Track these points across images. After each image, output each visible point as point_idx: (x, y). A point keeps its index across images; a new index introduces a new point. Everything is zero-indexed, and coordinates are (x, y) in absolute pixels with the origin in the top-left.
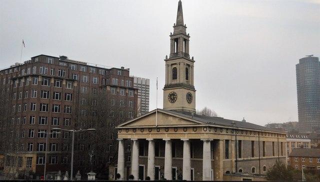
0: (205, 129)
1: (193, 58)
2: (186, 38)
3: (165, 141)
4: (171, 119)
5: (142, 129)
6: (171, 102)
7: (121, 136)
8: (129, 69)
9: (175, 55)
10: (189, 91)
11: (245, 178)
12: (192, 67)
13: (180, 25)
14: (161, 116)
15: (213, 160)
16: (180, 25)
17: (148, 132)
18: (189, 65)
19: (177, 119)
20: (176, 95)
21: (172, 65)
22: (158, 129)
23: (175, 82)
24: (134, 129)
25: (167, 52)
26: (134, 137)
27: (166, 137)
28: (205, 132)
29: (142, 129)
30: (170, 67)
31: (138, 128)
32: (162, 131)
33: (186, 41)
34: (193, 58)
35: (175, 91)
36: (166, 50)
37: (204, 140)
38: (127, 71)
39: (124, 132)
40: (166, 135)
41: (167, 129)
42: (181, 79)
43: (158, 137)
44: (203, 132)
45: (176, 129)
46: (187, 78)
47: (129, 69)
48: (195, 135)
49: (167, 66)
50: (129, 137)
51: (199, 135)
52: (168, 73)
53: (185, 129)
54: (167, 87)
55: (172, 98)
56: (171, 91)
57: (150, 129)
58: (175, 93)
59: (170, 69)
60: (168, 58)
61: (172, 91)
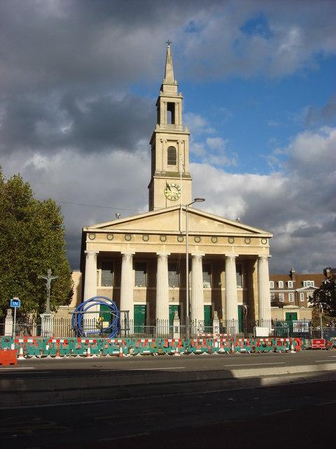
0: (264, 241)
17: (161, 243)
23: (173, 169)
24: (128, 234)
28: (263, 245)
43: (180, 250)
44: (261, 245)
48: (248, 250)
51: (256, 250)
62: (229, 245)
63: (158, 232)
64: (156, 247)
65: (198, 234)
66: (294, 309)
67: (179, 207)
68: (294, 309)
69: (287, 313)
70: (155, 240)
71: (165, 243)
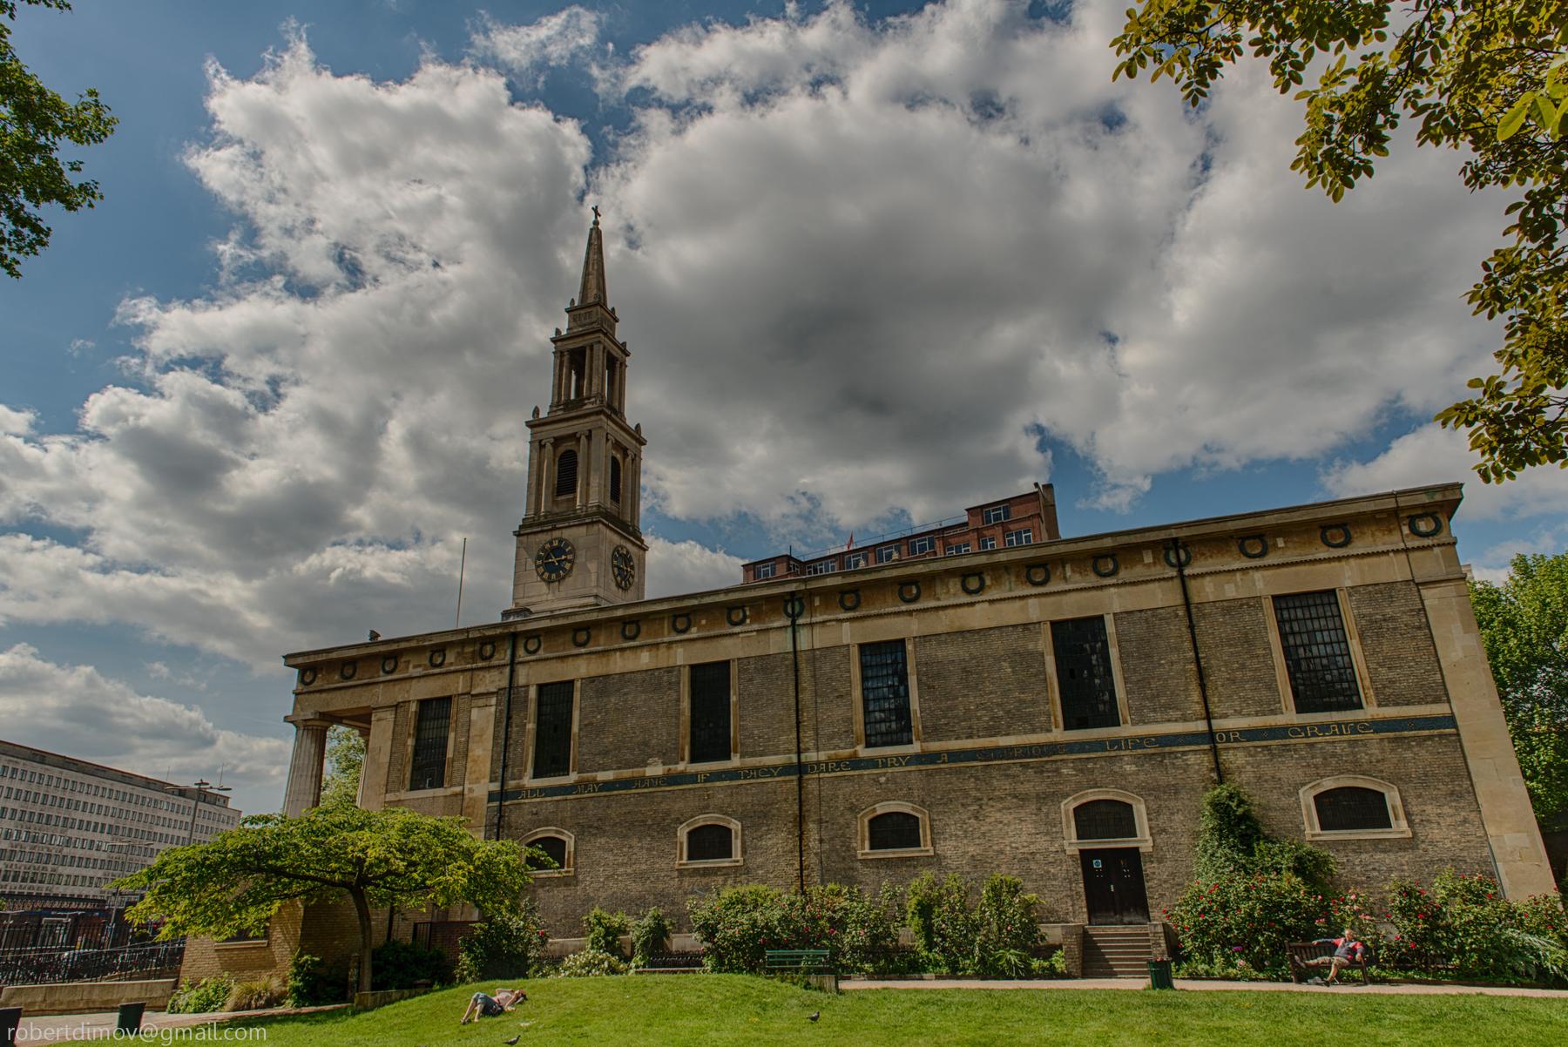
1: (638, 426)
2: (616, 352)
6: (549, 582)
9: (566, 406)
10: (623, 542)
12: (636, 459)
18: (625, 451)
20: (573, 552)
21: (558, 441)
33: (615, 364)
34: (638, 426)
35: (566, 534)
42: (593, 490)
46: (615, 495)
49: (538, 445)
52: (539, 484)
55: (554, 564)
58: (567, 545)
60: (543, 414)
61: (556, 534)
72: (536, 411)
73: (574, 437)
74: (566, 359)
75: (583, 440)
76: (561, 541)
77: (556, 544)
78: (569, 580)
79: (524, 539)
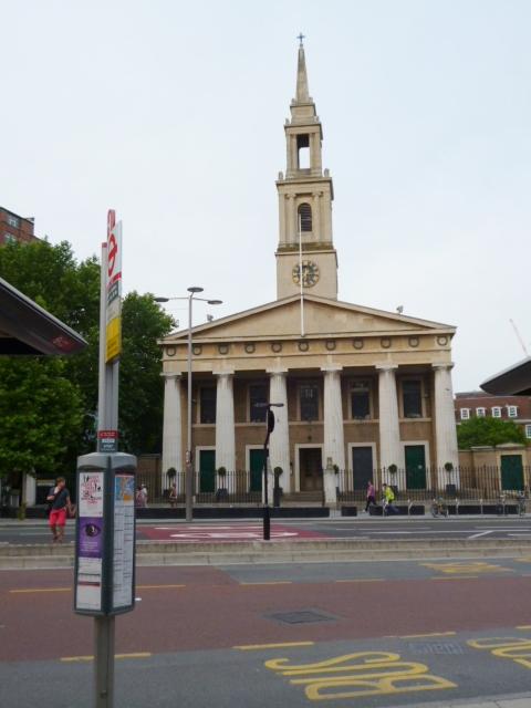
3: (325, 373)
4: (342, 317)
5: (247, 344)
7: (172, 367)
8: (33, 219)
11: (505, 453)
13: (302, 104)
14: (311, 310)
15: (429, 420)
16: (302, 104)
17: (273, 354)
19: (361, 319)
21: (299, 195)
22: (304, 342)
23: (303, 238)
24: (223, 346)
25: (281, 165)
26: (224, 367)
27: (331, 364)
28: (444, 348)
29: (250, 345)
30: (291, 199)
31: (236, 343)
32: (313, 349)
36: (275, 156)
37: (444, 365)
38: (29, 223)
39: (180, 354)
40: (330, 358)
41: (330, 342)
44: (437, 347)
45: (358, 341)
47: (33, 219)
50: (204, 367)
51: (428, 355)
53: (386, 340)
54: (284, 250)
56: (306, 258)
57: (277, 344)
59: (293, 206)
62: (385, 350)
63: (346, 336)
64: (267, 360)
65: (330, 336)
66: (515, 449)
67: (296, 298)
68: (515, 449)
69: (502, 457)
70: (266, 352)
71: (280, 354)
72: (280, 174)
73: (309, 195)
74: (295, 140)
75: (316, 198)
76: (309, 263)
77: (306, 264)
78: (317, 285)
79: (282, 258)
